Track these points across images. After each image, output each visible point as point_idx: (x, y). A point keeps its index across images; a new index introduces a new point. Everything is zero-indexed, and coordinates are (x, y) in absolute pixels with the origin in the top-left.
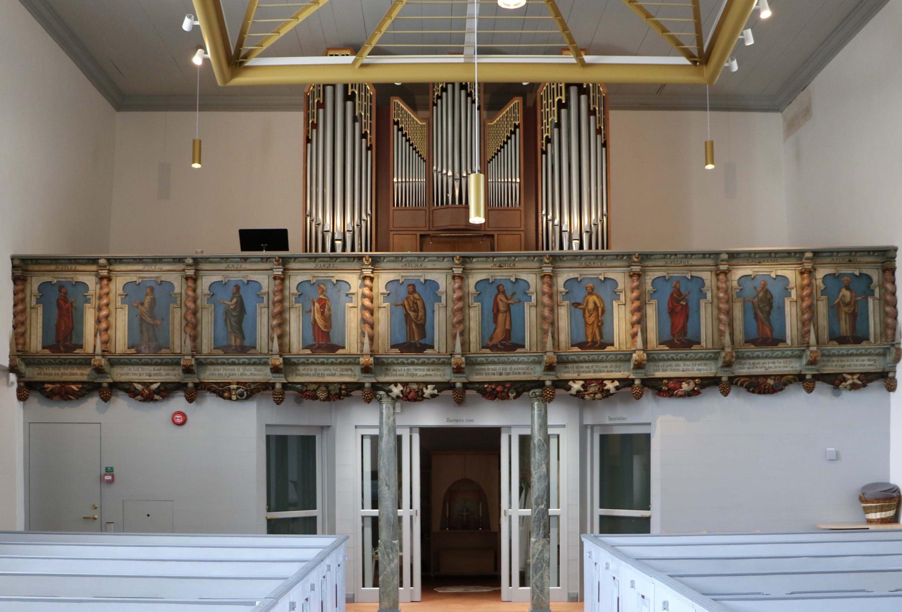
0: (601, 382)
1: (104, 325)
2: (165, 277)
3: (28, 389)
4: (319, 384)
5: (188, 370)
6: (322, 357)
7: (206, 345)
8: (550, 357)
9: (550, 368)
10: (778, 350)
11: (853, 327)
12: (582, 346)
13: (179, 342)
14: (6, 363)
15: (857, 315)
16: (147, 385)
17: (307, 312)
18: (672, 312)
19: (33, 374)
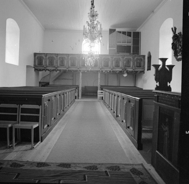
0: (107, 71)
1: (46, 62)
2: (53, 56)
3: (36, 70)
4: (72, 70)
5: (56, 68)
6: (73, 67)
7: (58, 65)
8: (101, 68)
9: (101, 69)
10: (129, 68)
11: (139, 65)
12: (105, 66)
13: (55, 64)
14: (33, 66)
15: (140, 64)
16: (51, 70)
17: (71, 61)
18: (116, 62)
19: (36, 68)
